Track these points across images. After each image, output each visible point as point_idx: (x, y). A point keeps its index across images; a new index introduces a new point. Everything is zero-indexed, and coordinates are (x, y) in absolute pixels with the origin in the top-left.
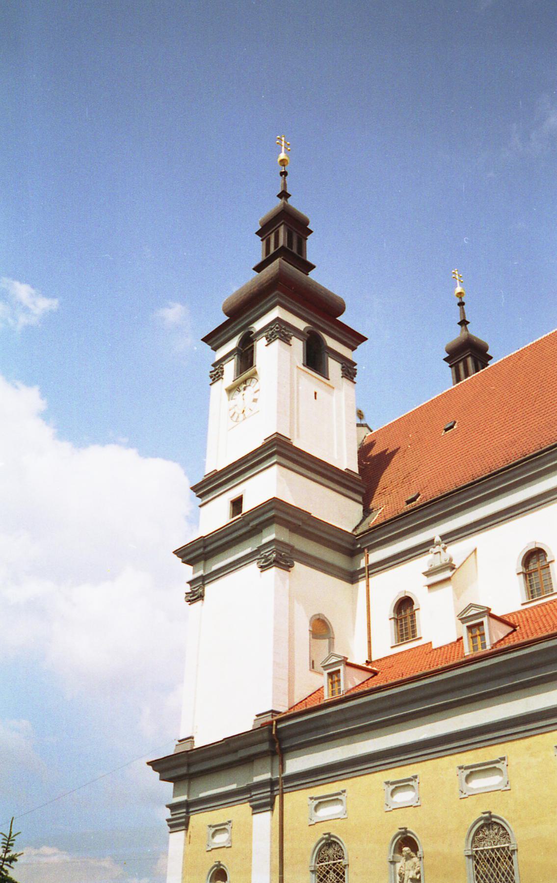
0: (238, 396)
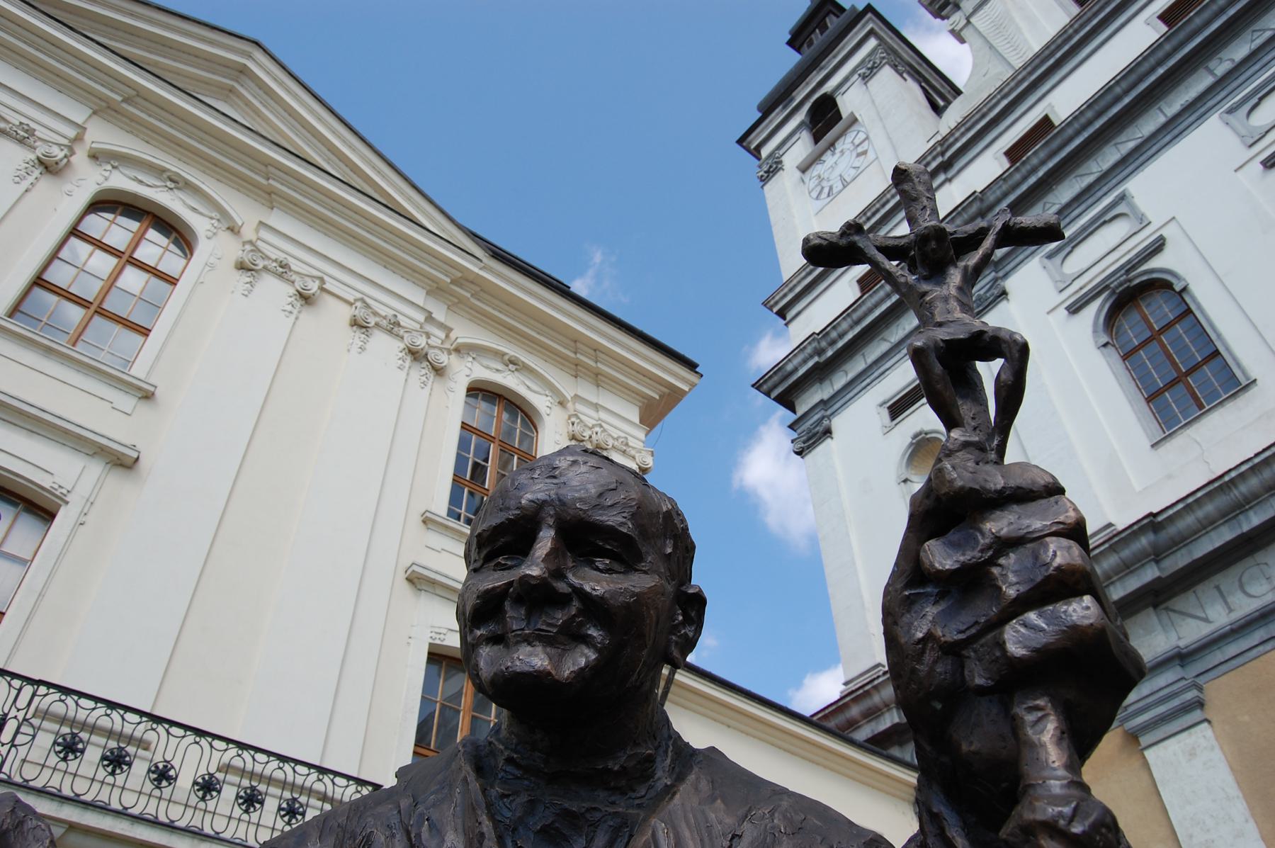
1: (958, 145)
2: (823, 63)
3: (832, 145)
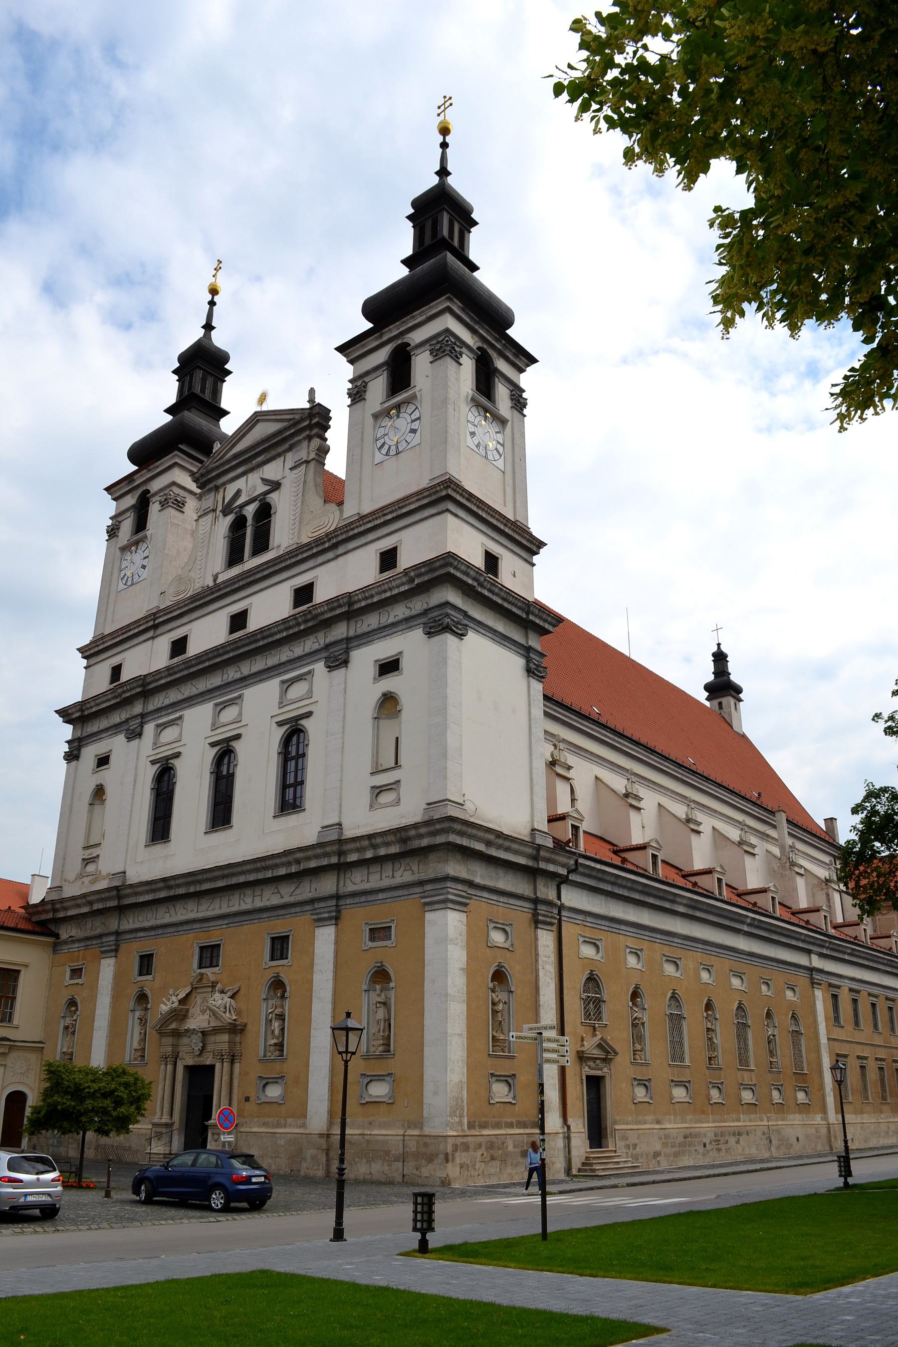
0: (128, 556)
1: (161, 620)
2: (151, 467)
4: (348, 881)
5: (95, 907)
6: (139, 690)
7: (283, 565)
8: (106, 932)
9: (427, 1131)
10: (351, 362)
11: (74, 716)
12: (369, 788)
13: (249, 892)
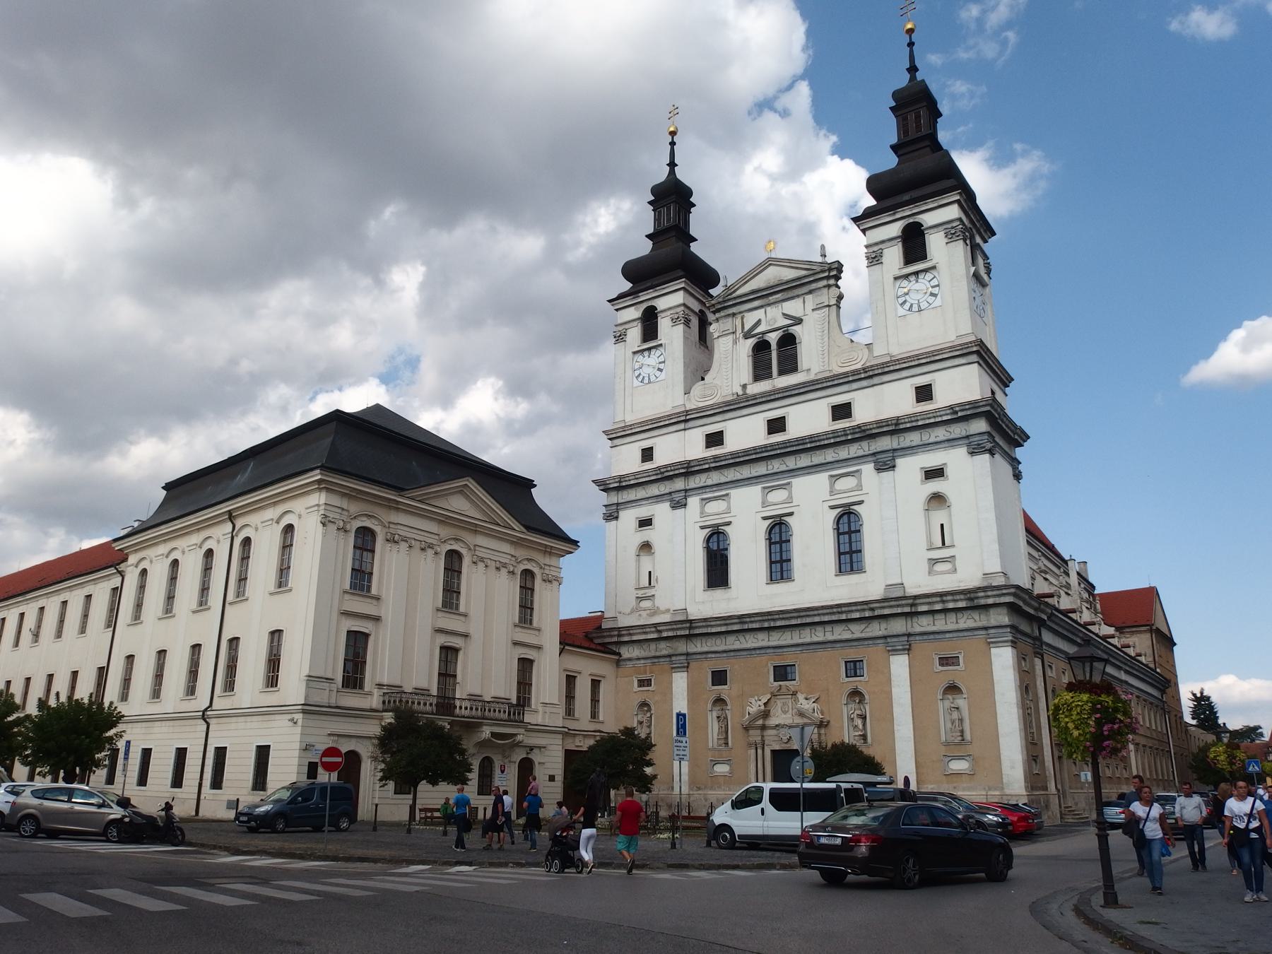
3: (649, 349)
4: (915, 624)
5: (665, 634)
6: (683, 471)
7: (820, 386)
8: (676, 653)
9: (1007, 792)
10: (864, 231)
11: (612, 486)
12: (926, 561)
13: (819, 629)
